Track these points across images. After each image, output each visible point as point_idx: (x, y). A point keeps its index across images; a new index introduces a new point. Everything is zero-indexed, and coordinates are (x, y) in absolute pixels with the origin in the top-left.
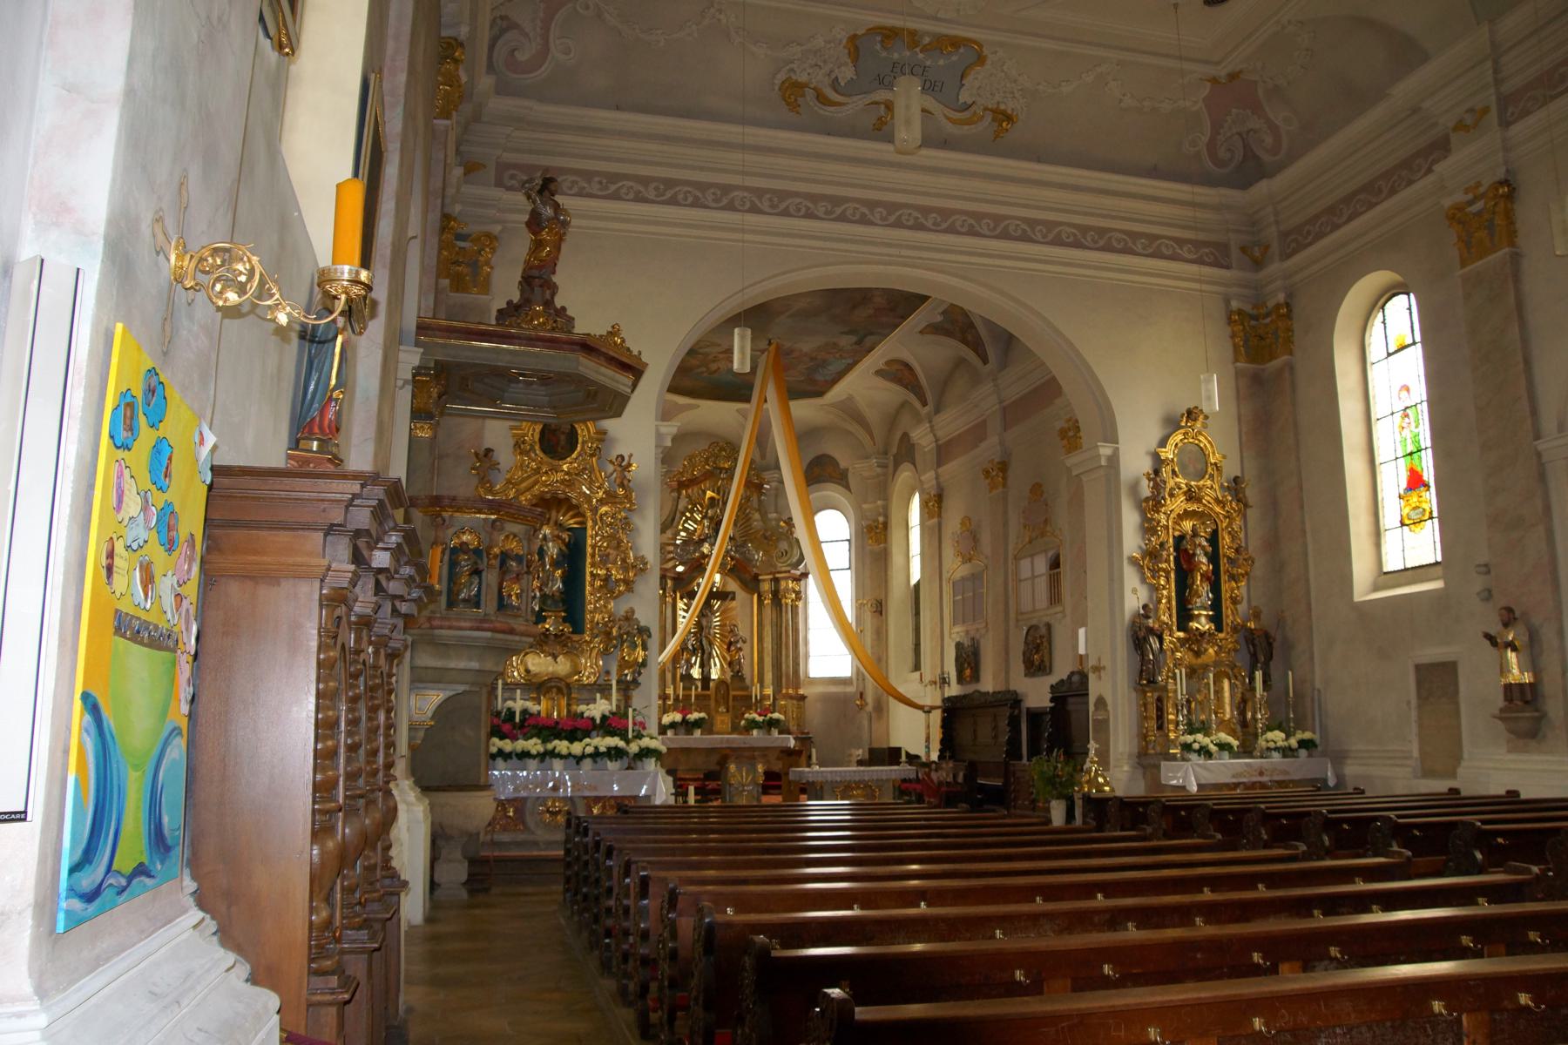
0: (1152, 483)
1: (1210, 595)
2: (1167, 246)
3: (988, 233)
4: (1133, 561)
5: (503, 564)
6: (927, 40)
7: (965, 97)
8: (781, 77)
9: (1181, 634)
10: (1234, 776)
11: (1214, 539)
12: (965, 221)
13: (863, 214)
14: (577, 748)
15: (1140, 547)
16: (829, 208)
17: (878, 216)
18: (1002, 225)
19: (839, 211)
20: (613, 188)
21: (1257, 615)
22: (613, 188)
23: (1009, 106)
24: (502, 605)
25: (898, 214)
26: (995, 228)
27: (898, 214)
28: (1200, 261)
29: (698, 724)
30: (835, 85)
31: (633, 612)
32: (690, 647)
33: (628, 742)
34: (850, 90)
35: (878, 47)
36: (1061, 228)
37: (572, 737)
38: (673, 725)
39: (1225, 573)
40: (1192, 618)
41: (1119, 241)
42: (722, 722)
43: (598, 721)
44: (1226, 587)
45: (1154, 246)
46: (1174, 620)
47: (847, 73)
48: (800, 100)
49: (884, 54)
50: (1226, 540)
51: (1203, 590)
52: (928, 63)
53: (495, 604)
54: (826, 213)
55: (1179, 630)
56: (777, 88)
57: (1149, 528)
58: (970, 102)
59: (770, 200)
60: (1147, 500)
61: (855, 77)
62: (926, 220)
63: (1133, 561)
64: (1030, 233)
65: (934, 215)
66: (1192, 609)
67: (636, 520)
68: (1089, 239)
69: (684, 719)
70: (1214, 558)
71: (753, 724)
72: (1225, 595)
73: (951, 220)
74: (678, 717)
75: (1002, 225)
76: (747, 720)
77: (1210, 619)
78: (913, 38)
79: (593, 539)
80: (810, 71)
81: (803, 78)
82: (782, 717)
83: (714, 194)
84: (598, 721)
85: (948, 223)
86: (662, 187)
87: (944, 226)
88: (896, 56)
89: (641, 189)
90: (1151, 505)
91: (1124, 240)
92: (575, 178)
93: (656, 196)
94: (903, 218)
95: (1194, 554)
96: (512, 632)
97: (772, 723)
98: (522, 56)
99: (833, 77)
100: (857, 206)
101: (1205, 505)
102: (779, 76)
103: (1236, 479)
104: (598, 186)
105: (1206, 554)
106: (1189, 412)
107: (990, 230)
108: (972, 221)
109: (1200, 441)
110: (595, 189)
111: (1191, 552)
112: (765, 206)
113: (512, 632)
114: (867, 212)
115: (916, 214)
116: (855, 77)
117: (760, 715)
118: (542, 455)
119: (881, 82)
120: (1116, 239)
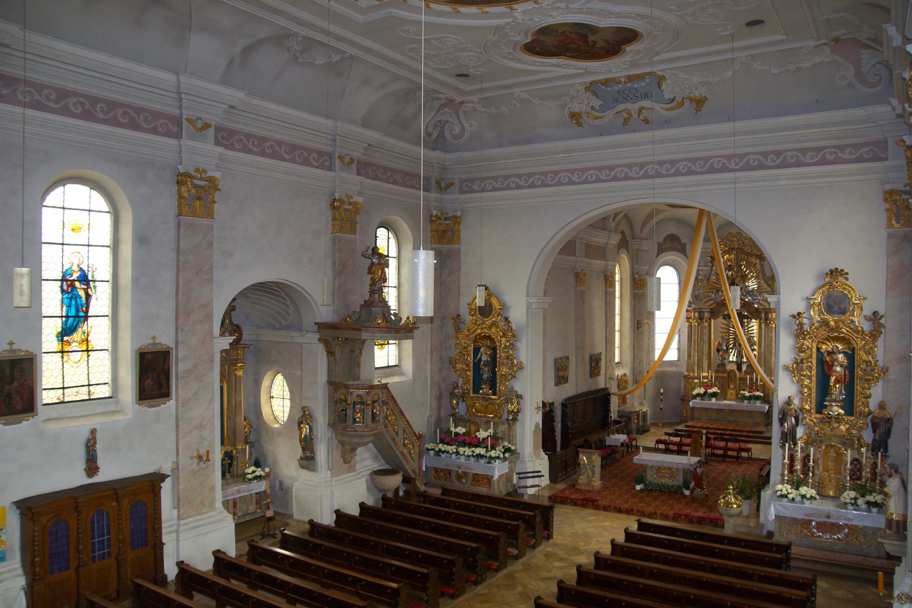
0: (797, 322)
1: (843, 392)
2: (831, 154)
3: (699, 170)
4: (786, 368)
5: (354, 407)
6: (623, 80)
7: (667, 96)
8: (566, 112)
9: (818, 416)
10: (806, 515)
11: (851, 357)
12: (685, 165)
13: (626, 173)
14: (468, 451)
15: (792, 360)
16: (608, 172)
17: (634, 172)
18: (710, 163)
19: (613, 174)
20: (506, 183)
21: (882, 406)
22: (506, 183)
23: (696, 94)
24: (355, 421)
25: (646, 168)
26: (704, 166)
27: (646, 168)
28: (860, 160)
29: (714, 395)
30: (593, 108)
31: (512, 388)
32: (725, 348)
33: (487, 451)
34: (603, 108)
35: (603, 87)
36: (748, 158)
37: (471, 445)
38: (698, 395)
39: (857, 378)
40: (826, 406)
41: (791, 157)
42: (731, 394)
43: (481, 440)
44: (858, 387)
45: (820, 155)
46: (813, 406)
47: (597, 103)
48: (581, 120)
49: (609, 89)
50: (861, 355)
51: (837, 390)
52: (636, 86)
53: (351, 421)
54: (607, 176)
55: (817, 413)
56: (567, 117)
57: (800, 350)
58: (672, 97)
59: (578, 174)
60: (797, 330)
61: (602, 103)
62: (662, 169)
63: (786, 368)
64: (727, 165)
65: (666, 165)
66: (826, 401)
67: (518, 344)
68: (769, 160)
69: (706, 393)
70: (851, 366)
71: (744, 398)
72: (856, 393)
73: (677, 166)
74: (702, 391)
75: (710, 163)
76: (742, 394)
77: (842, 408)
78: (615, 81)
79: (501, 354)
80: (579, 106)
81: (576, 110)
82: (762, 394)
83: (551, 177)
84: (481, 440)
85: (675, 168)
86: (527, 178)
87: (673, 170)
88: (616, 88)
89: (518, 180)
90: (800, 333)
91: (795, 155)
92: (491, 181)
93: (526, 183)
94: (649, 171)
95: (833, 365)
96: (356, 431)
97: (757, 398)
98: (457, 131)
99: (590, 106)
100: (623, 169)
101: (843, 333)
102: (565, 112)
103: (875, 313)
104: (500, 183)
105: (842, 366)
106: (831, 271)
107: (701, 168)
108: (689, 164)
109: (844, 289)
110: (499, 185)
111: (830, 363)
112: (575, 179)
113: (356, 431)
114: (629, 171)
115: (656, 167)
116: (602, 103)
117: (749, 392)
118: (479, 316)
119: (617, 101)
120: (790, 157)
